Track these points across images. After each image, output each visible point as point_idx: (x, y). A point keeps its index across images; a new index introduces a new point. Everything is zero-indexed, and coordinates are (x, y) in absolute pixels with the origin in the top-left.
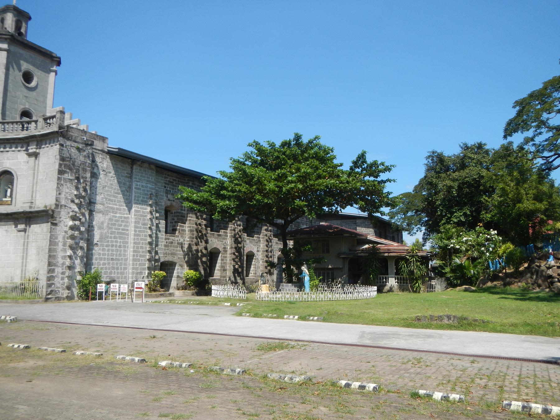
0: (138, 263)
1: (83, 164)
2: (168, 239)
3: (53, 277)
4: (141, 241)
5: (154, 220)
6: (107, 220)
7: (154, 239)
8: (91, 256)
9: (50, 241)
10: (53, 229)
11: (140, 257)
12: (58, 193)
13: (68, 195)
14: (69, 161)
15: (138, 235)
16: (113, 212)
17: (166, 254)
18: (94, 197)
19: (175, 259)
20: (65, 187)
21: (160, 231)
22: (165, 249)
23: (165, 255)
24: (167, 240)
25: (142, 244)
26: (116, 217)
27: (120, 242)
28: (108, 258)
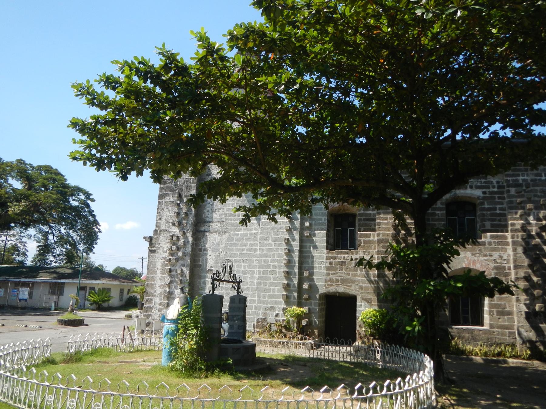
0: (267, 294)
1: (187, 181)
2: (335, 258)
3: (150, 307)
4: (272, 264)
5: (294, 232)
6: (225, 240)
7: (297, 259)
8: (202, 285)
9: (148, 269)
10: (151, 257)
11: (270, 286)
12: (158, 218)
13: (169, 219)
14: (171, 182)
15: (266, 256)
16: (234, 230)
17: (331, 280)
18: (209, 216)
19: (352, 290)
20: (166, 210)
21: (315, 247)
22: (328, 274)
23: (329, 283)
24: (332, 260)
25: (274, 267)
26: (238, 235)
27: (245, 267)
28: (226, 288)
